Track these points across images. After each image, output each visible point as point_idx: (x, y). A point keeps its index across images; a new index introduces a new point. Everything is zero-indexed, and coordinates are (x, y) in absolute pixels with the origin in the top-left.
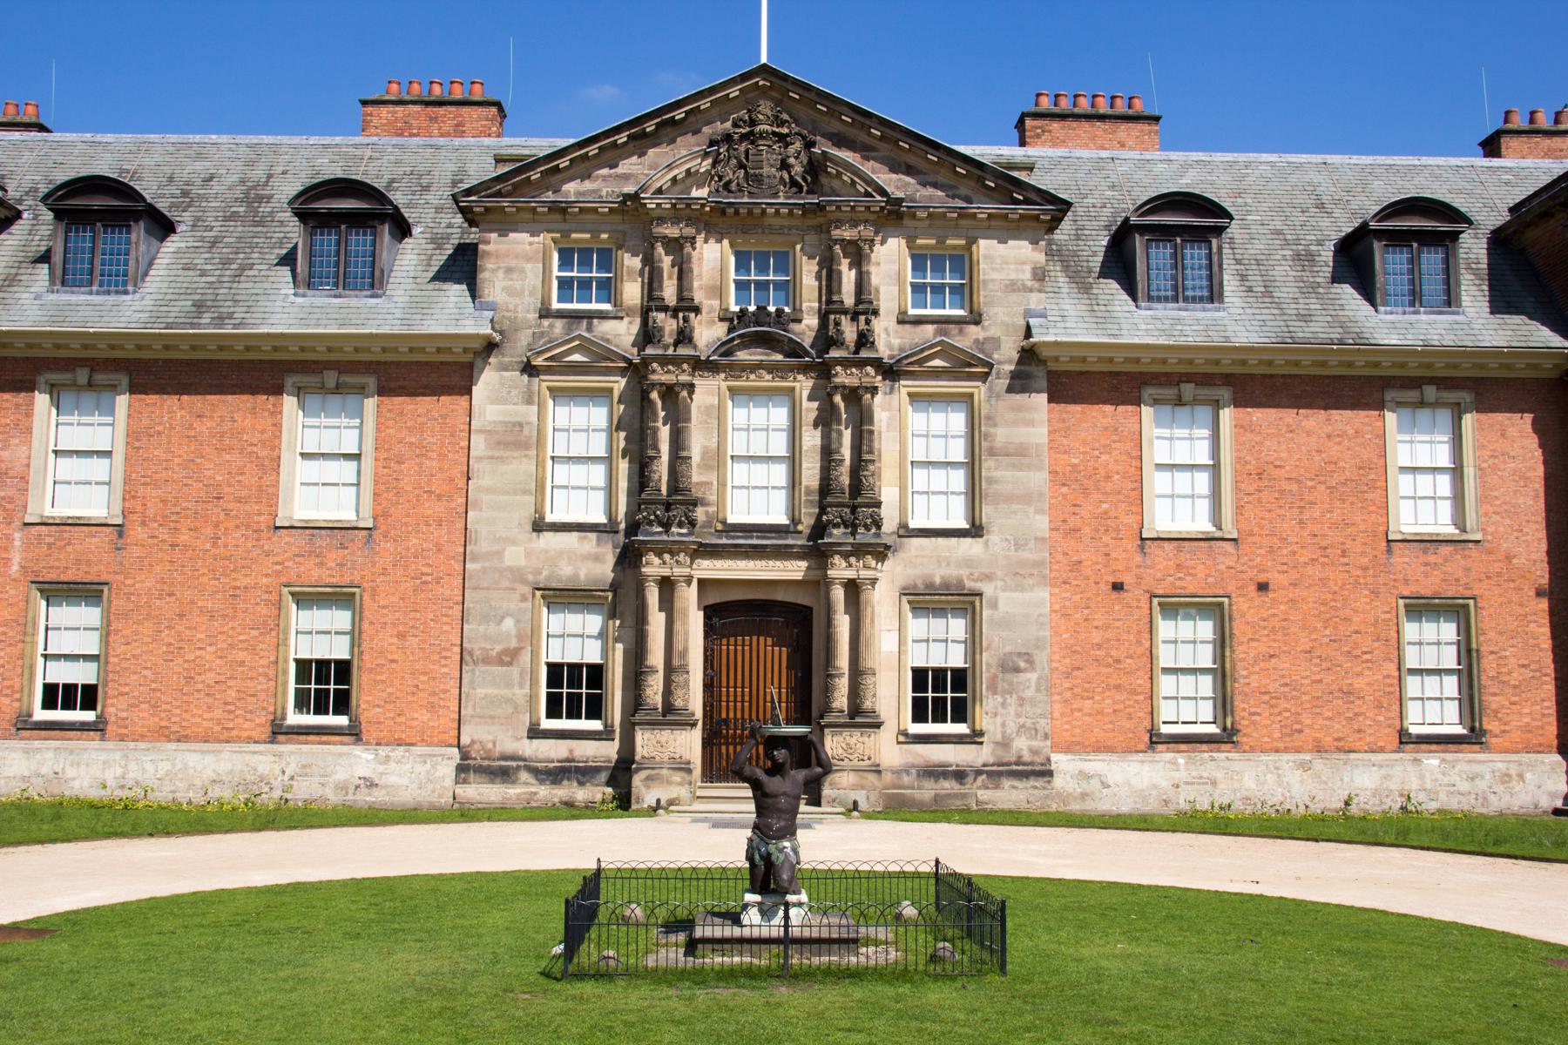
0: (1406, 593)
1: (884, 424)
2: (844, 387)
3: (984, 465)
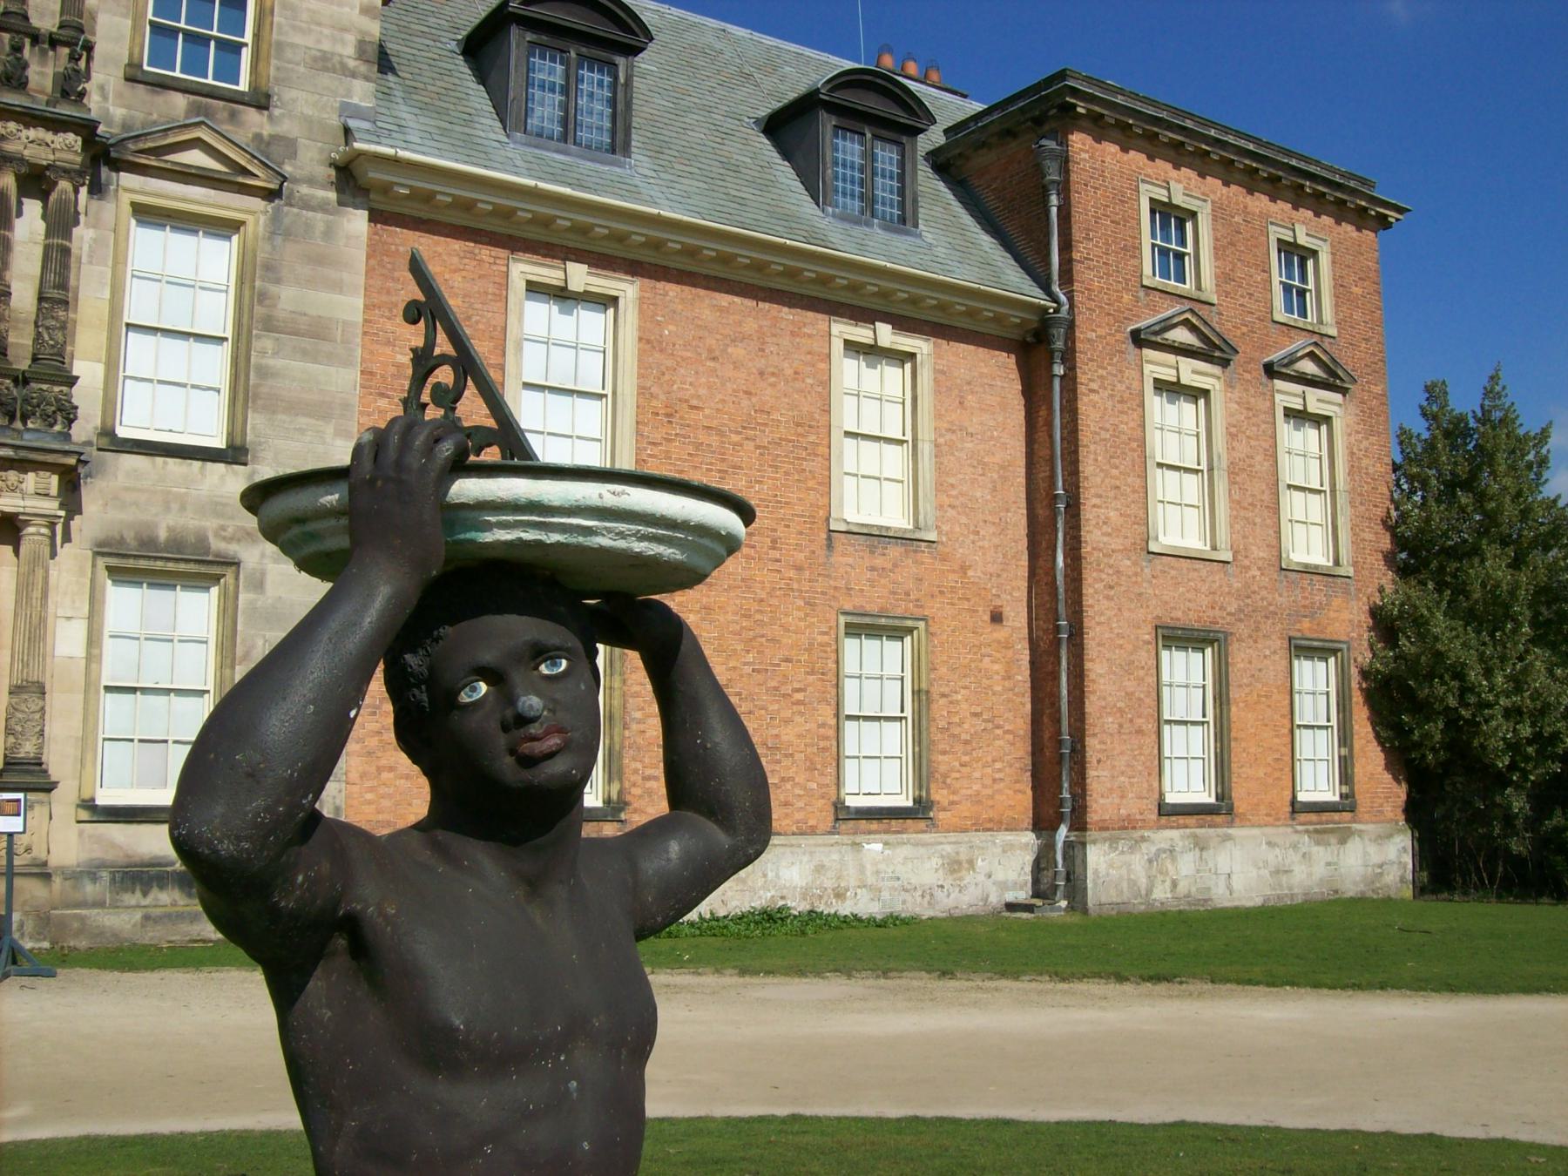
0: (848, 607)
1: (86, 248)
2: (21, 160)
3: (256, 345)
